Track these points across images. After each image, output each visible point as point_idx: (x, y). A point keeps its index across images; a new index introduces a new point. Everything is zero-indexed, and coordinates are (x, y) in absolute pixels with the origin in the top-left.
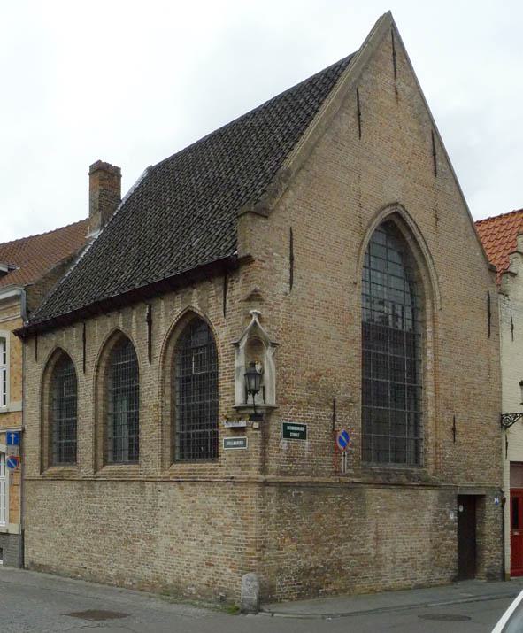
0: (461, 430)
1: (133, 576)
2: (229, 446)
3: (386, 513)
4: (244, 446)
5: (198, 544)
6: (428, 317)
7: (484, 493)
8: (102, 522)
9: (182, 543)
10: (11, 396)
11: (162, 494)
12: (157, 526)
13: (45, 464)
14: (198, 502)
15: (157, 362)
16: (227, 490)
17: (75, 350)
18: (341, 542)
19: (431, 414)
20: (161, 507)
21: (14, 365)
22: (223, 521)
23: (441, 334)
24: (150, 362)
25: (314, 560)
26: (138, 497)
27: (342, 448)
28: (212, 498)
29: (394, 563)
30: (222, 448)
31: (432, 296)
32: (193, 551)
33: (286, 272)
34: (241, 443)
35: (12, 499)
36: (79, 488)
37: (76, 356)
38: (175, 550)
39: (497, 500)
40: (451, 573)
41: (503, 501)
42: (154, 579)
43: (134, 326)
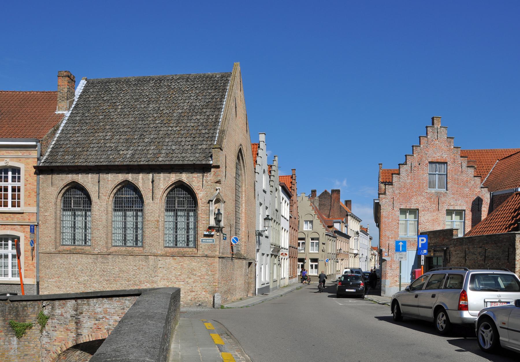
2: (204, 242)
4: (213, 242)
8: (115, 276)
9: (175, 283)
10: (25, 203)
11: (161, 262)
12: (158, 276)
14: (185, 265)
16: (203, 260)
17: (89, 185)
20: (160, 267)
22: (200, 273)
26: (144, 263)
28: (194, 264)
34: (211, 241)
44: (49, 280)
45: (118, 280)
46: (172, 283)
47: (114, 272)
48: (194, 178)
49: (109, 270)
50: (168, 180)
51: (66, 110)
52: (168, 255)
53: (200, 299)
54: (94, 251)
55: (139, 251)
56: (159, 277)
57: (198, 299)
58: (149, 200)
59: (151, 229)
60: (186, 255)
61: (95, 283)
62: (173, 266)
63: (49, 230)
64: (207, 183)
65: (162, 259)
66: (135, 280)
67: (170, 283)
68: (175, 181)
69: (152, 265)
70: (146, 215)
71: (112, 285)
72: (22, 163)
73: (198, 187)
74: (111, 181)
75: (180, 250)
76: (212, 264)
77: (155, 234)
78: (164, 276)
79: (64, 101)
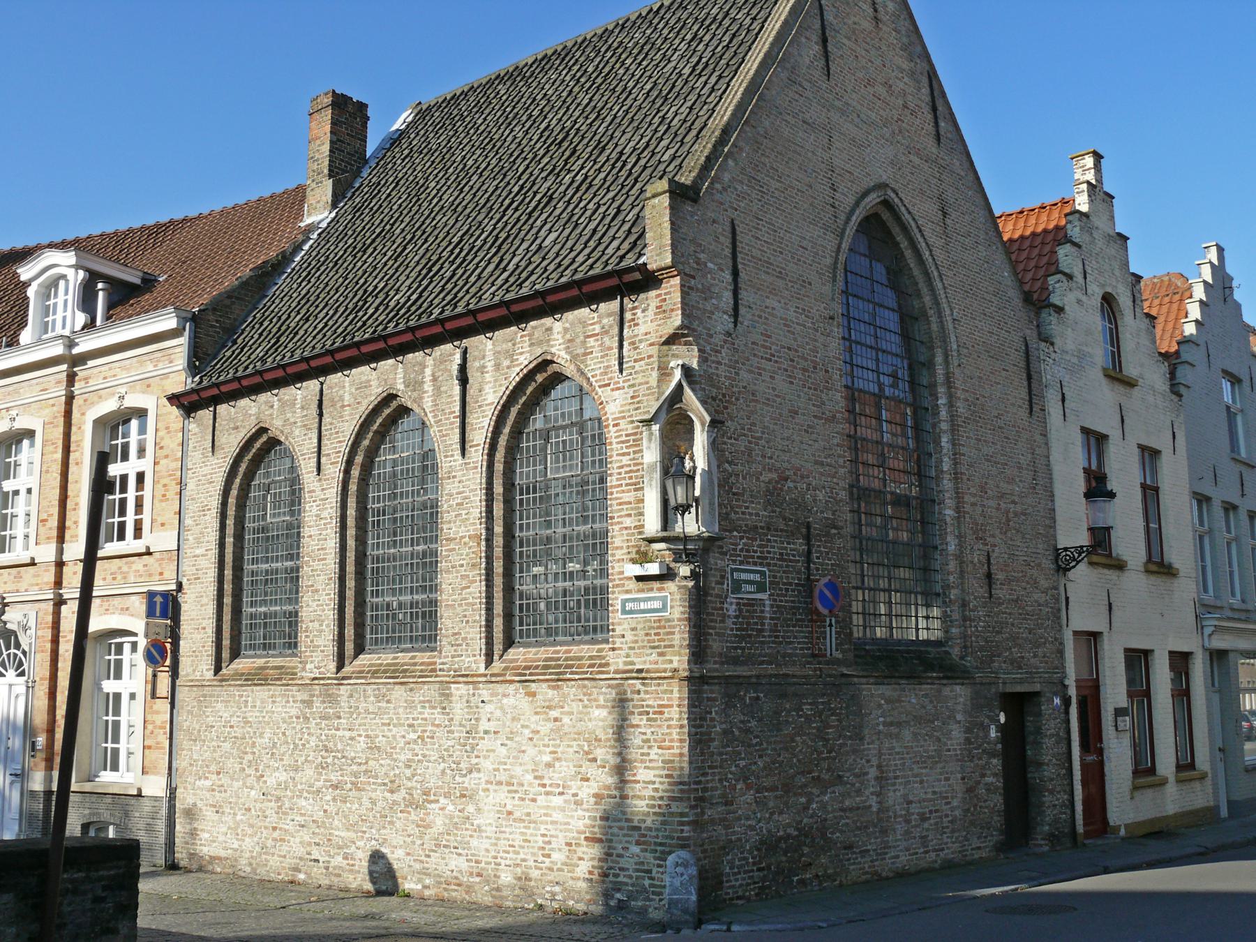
0: (1000, 576)
1: (425, 872)
2: (631, 612)
3: (894, 730)
5: (565, 801)
6: (940, 378)
7: (1037, 688)
8: (355, 768)
9: (534, 800)
11: (489, 708)
12: (479, 771)
13: (226, 654)
14: (566, 720)
15: (477, 455)
17: (297, 432)
18: (824, 786)
19: (952, 548)
20: (486, 732)
21: (163, 462)
23: (961, 408)
24: (463, 454)
25: (784, 822)
27: (825, 611)
29: (908, 821)
30: (616, 617)
31: (945, 339)
32: (557, 816)
33: (728, 296)
35: (150, 727)
36: (303, 702)
37: (301, 443)
38: (517, 814)
39: (1057, 701)
40: (996, 837)
41: (1067, 702)
42: (471, 874)
43: (428, 387)
44: (197, 782)
45: (365, 783)
46: (523, 799)
47: (353, 754)
48: (592, 339)
49: (340, 747)
50: (508, 367)
51: (325, 209)
52: (508, 678)
53: (621, 879)
54: (304, 674)
55: (288, 685)
56: (481, 775)
57: (616, 876)
58: (452, 456)
59: (457, 572)
60: (568, 676)
61: (305, 794)
62: (527, 727)
63: (202, 606)
64: (635, 349)
65: (492, 695)
66: (409, 784)
67: (517, 802)
68: (531, 366)
69: (461, 725)
70: (442, 518)
71: (348, 805)
72: (152, 393)
73: (606, 373)
74: (349, 405)
75: (558, 652)
76: (661, 713)
77: (470, 594)
78: (498, 770)
79: (321, 182)
